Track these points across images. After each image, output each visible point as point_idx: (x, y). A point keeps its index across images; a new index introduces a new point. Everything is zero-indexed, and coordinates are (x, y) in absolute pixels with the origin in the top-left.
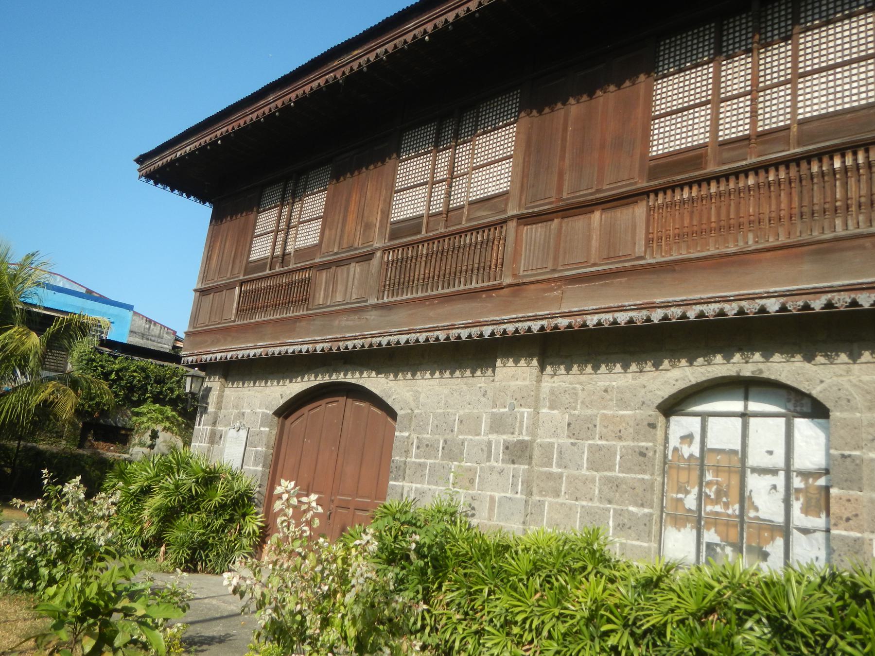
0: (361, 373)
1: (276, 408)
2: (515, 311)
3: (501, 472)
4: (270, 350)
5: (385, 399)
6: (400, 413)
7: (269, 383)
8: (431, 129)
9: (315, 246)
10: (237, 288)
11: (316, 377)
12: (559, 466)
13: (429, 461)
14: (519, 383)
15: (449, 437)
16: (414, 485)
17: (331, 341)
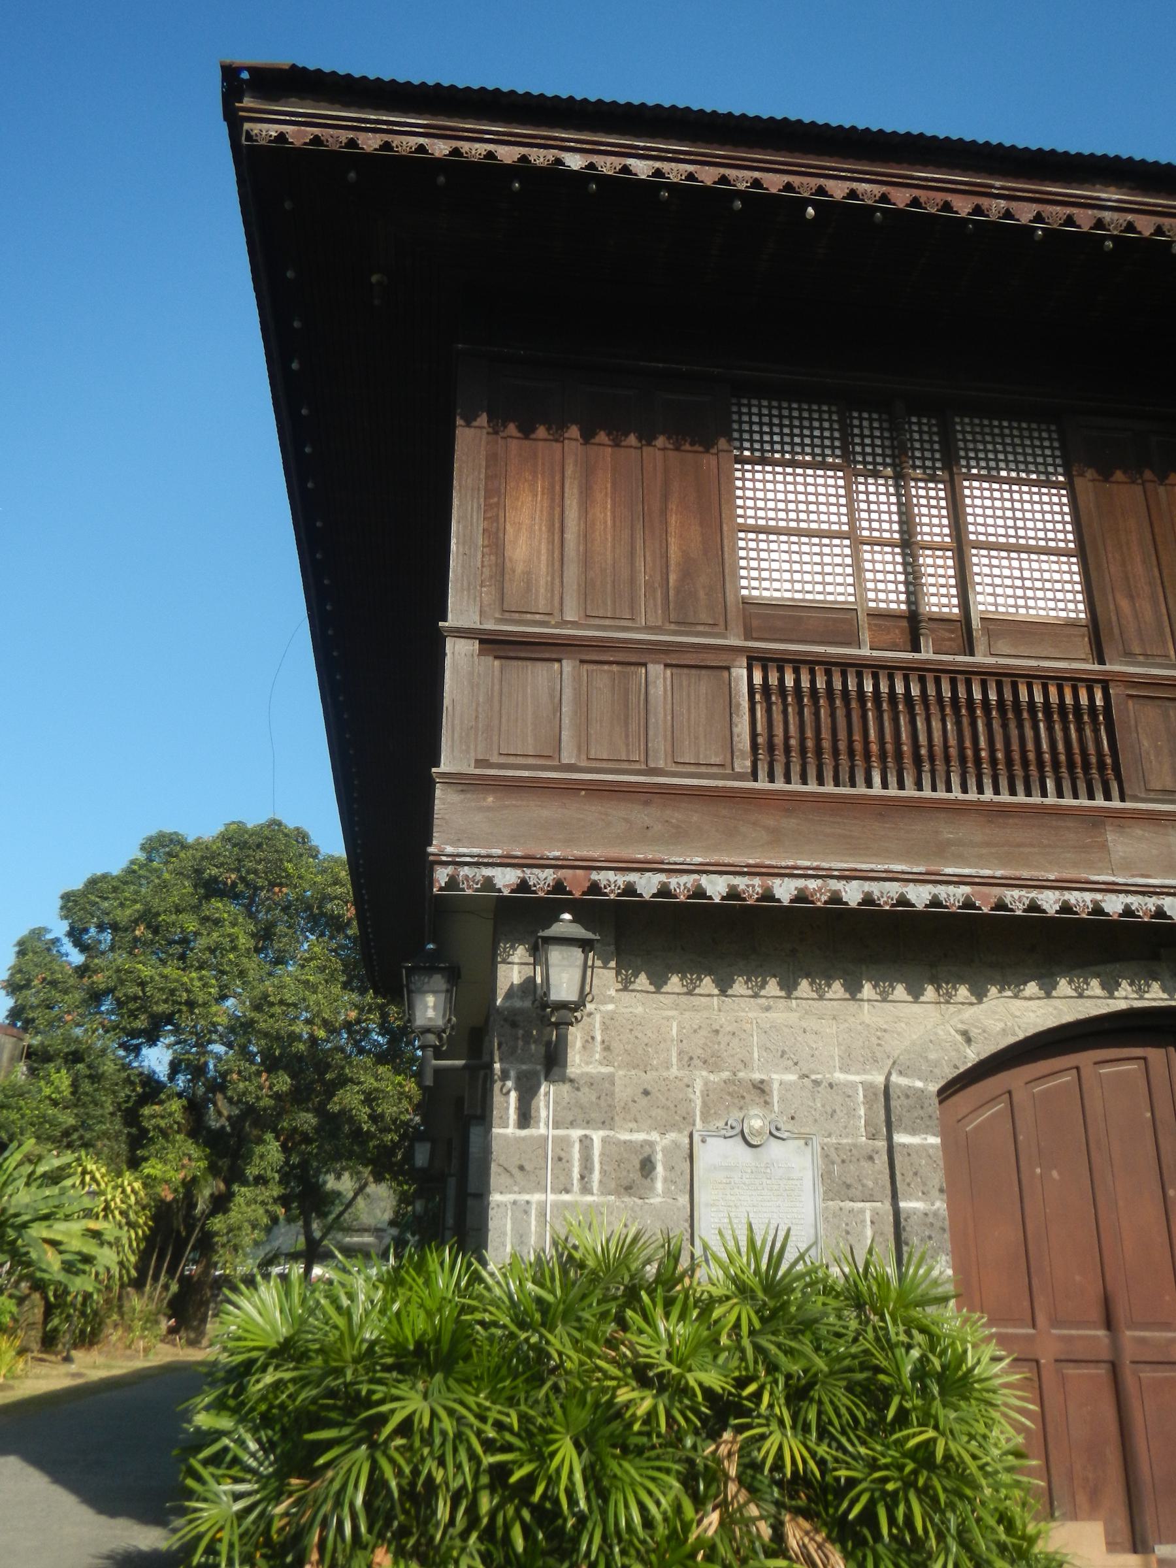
1: (951, 1073)
4: (1017, 899)
7: (868, 991)
9: (1071, 624)
10: (740, 673)
11: (1110, 987)
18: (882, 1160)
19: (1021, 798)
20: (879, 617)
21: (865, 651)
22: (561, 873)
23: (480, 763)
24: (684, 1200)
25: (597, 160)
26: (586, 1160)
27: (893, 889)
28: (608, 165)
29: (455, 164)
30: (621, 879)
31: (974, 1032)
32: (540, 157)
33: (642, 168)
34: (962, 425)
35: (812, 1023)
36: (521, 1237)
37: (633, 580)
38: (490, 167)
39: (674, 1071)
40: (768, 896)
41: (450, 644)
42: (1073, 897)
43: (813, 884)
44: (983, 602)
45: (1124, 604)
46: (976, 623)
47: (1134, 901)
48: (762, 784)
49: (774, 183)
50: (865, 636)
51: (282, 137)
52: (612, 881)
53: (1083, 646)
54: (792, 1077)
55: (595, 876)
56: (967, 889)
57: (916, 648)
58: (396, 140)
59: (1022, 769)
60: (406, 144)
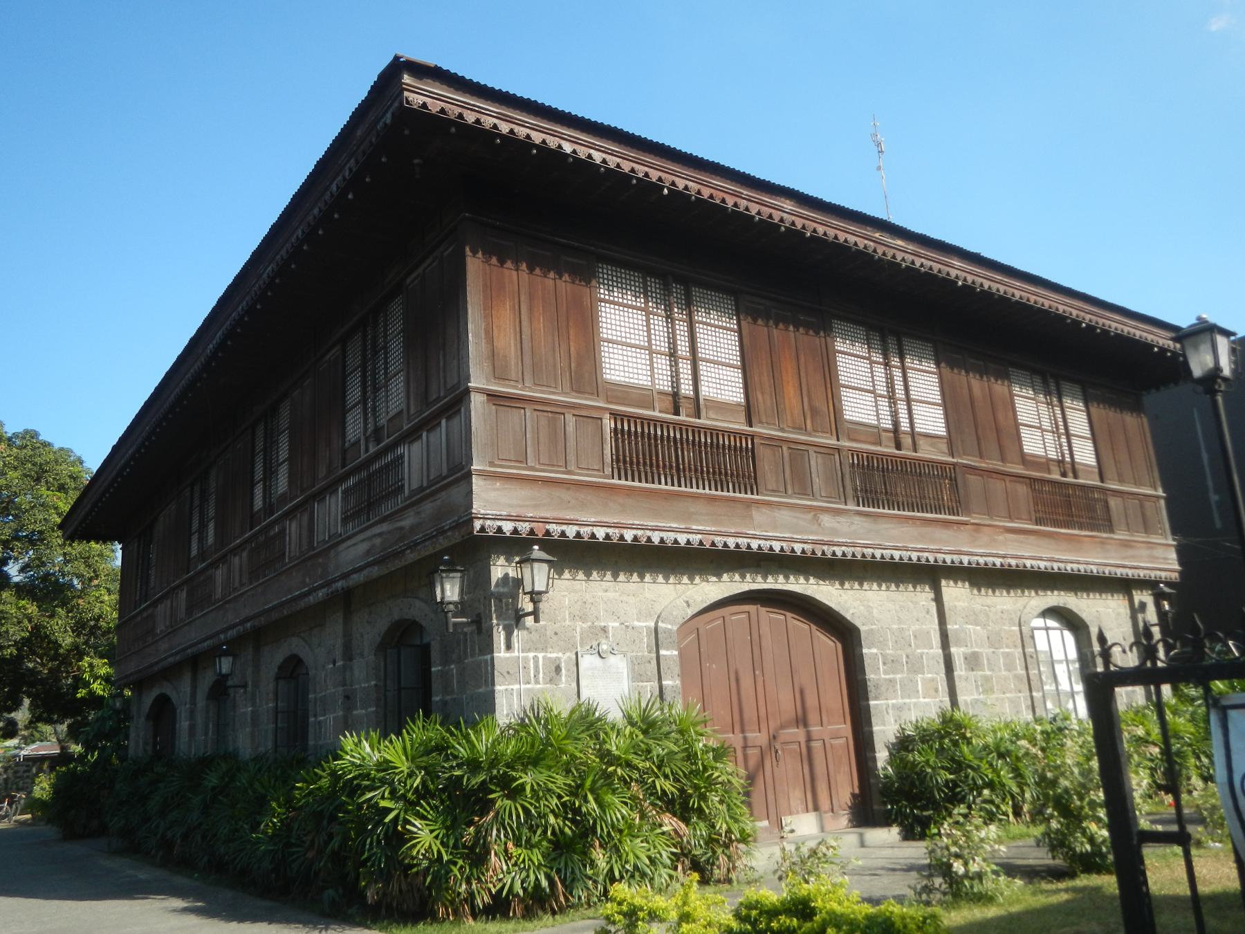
0: (807, 580)
1: (681, 621)
2: (980, 547)
3: (967, 679)
5: (842, 613)
6: (863, 629)
8: (861, 332)
9: (739, 404)
12: (990, 669)
13: (898, 676)
14: (961, 603)
15: (909, 651)
16: (890, 702)
17: (815, 543)
18: (655, 662)
19: (719, 493)
20: (661, 393)
21: (656, 414)
22: (533, 525)
23: (492, 464)
24: (574, 685)
25: (577, 147)
26: (536, 667)
27: (672, 536)
28: (583, 153)
29: (510, 139)
30: (559, 528)
31: (691, 602)
32: (552, 142)
33: (598, 157)
34: (695, 291)
35: (624, 598)
36: (511, 706)
37: (555, 365)
38: (527, 144)
39: (567, 623)
40: (622, 538)
41: (473, 395)
42: (740, 541)
43: (640, 533)
44: (705, 391)
45: (760, 396)
46: (702, 402)
47: (762, 543)
48: (616, 481)
49: (654, 175)
50: (657, 405)
51: (424, 105)
52: (555, 529)
53: (742, 417)
54: (617, 624)
55: (548, 527)
56: (699, 536)
57: (677, 413)
58: (483, 118)
59: (719, 478)
60: (488, 122)
